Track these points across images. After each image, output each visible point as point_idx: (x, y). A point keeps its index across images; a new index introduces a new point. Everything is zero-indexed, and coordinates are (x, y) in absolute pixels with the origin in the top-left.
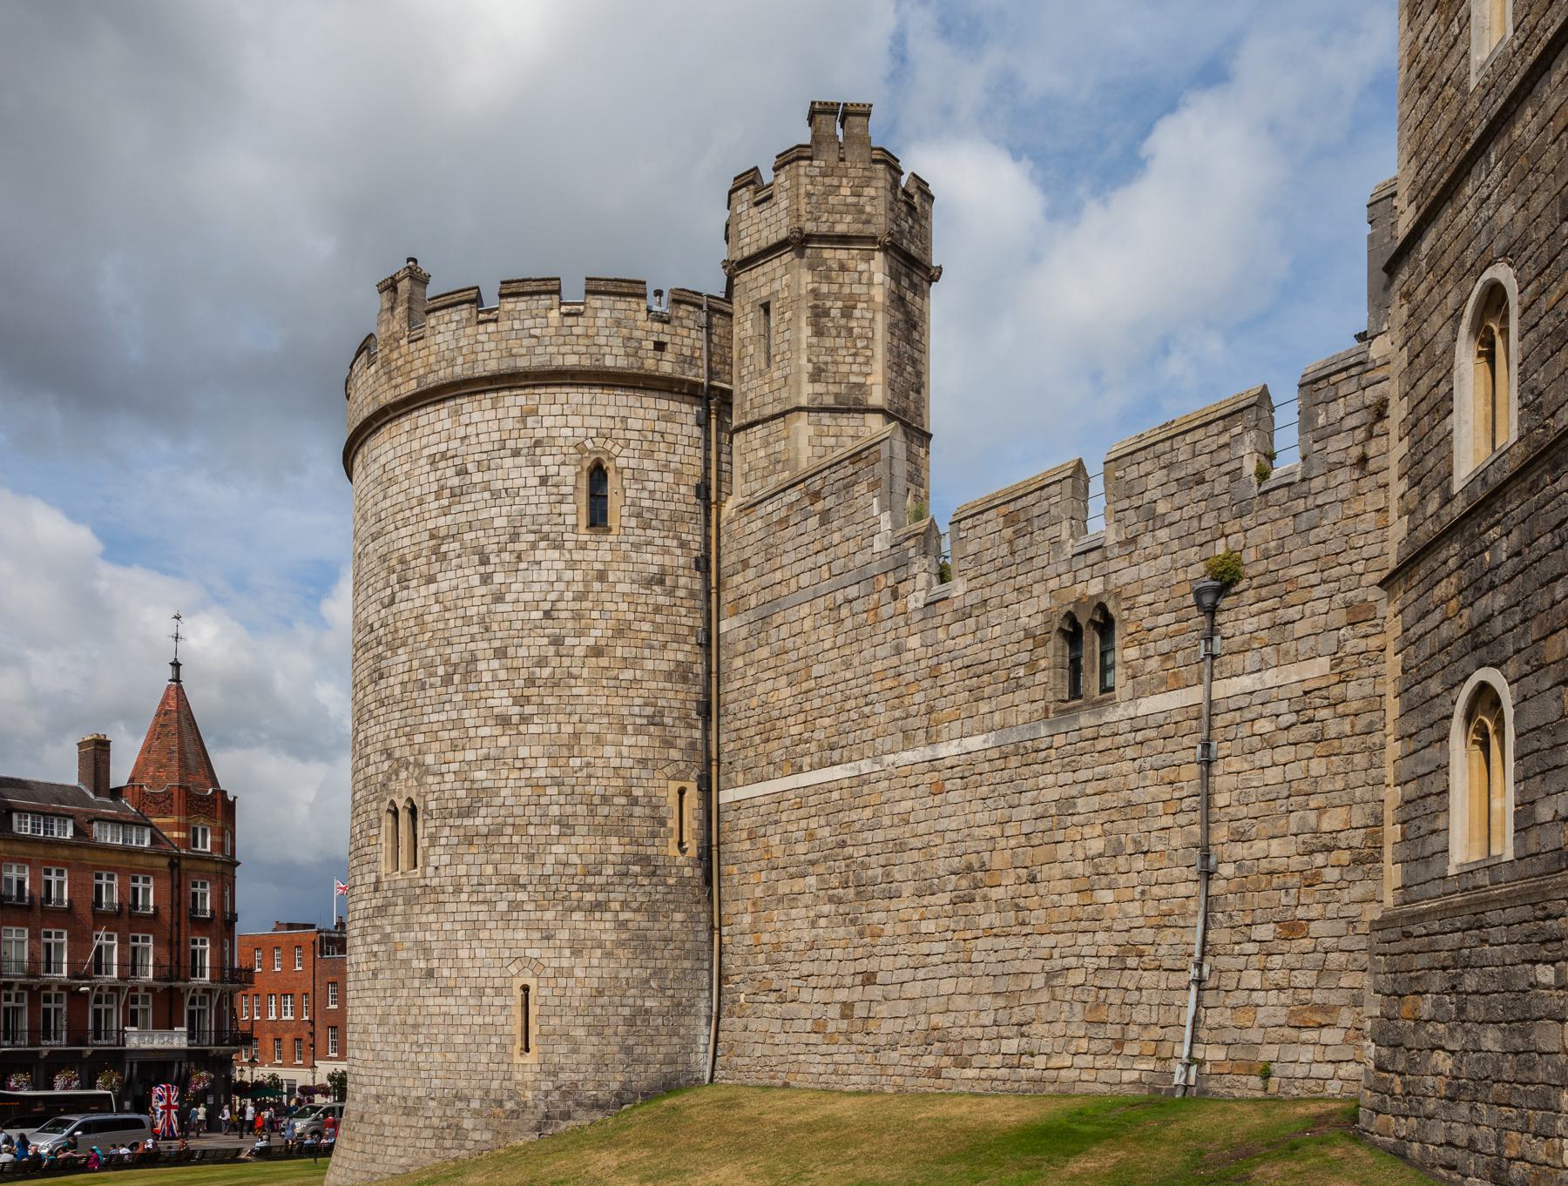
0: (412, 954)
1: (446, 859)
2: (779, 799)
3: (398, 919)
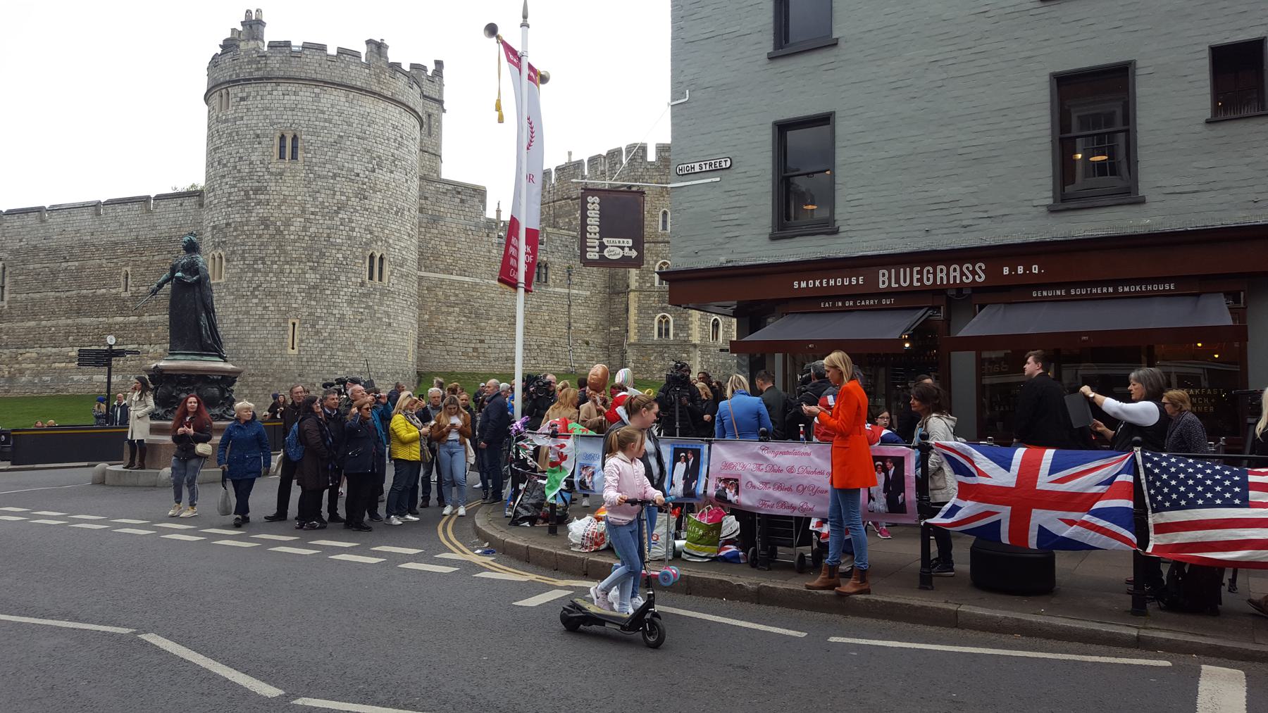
1: (396, 282)
2: (443, 280)
3: (376, 300)
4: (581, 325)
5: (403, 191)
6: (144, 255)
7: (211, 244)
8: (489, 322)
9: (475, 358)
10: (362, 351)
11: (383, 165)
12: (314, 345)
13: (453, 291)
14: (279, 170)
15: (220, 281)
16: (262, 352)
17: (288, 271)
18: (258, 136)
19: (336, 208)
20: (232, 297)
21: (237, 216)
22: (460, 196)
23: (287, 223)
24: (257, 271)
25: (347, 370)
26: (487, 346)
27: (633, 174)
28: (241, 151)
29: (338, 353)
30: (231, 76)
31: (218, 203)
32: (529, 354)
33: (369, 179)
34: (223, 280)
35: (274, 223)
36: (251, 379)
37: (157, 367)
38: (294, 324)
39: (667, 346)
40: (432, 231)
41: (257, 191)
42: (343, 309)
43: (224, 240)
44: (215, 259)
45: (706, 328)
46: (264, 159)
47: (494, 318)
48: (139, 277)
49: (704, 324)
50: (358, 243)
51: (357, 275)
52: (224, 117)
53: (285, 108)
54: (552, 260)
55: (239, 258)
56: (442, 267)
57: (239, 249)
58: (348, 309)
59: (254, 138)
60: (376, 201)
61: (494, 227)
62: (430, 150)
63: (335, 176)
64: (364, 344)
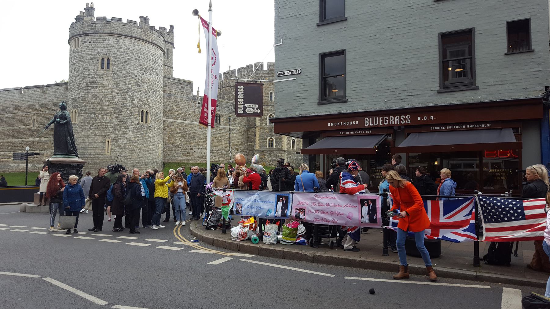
0: (148, 138)
2: (174, 122)
4: (235, 142)
5: (156, 83)
6: (42, 111)
7: (71, 106)
8: (195, 140)
9: (188, 156)
10: (139, 153)
11: (147, 71)
12: (117, 151)
13: (178, 127)
15: (75, 123)
16: (95, 154)
17: (105, 118)
18: (92, 59)
20: (81, 130)
21: (83, 94)
22: (181, 85)
23: (105, 97)
25: (132, 161)
26: (193, 151)
27: (257, 76)
28: (84, 65)
29: (128, 154)
30: (80, 32)
32: (212, 155)
33: (141, 78)
34: (77, 122)
35: (99, 97)
36: (89, 166)
37: (48, 160)
38: (108, 141)
39: (272, 151)
40: (169, 100)
42: (130, 135)
43: (77, 104)
44: (73, 113)
45: (289, 143)
46: (94, 69)
47: (197, 139)
48: (40, 121)
49: (288, 141)
50: (136, 106)
51: (136, 120)
52: (77, 50)
53: (104, 46)
54: (222, 113)
56: (173, 116)
57: (84, 109)
58: (132, 135)
59: (90, 60)
60: (144, 87)
61: (196, 99)
62: (168, 65)
63: (126, 76)
64: (139, 150)
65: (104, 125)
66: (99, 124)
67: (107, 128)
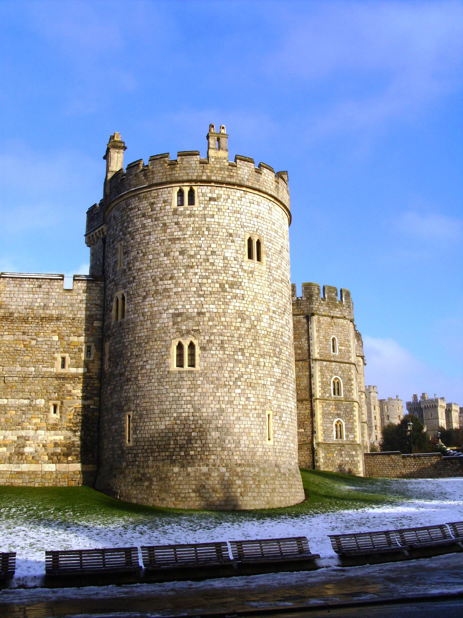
14: (250, 269)
16: (247, 442)
17: (263, 364)
18: (231, 235)
19: (283, 310)
20: (213, 386)
21: (211, 306)
24: (237, 361)
28: (213, 245)
31: (183, 291)
34: (198, 368)
35: (249, 317)
36: (239, 469)
38: (269, 416)
39: (343, 445)
41: (232, 285)
43: (194, 328)
46: (237, 257)
52: (188, 212)
55: (219, 348)
59: (226, 236)
65: (262, 378)
66: (253, 377)
67: (267, 386)
